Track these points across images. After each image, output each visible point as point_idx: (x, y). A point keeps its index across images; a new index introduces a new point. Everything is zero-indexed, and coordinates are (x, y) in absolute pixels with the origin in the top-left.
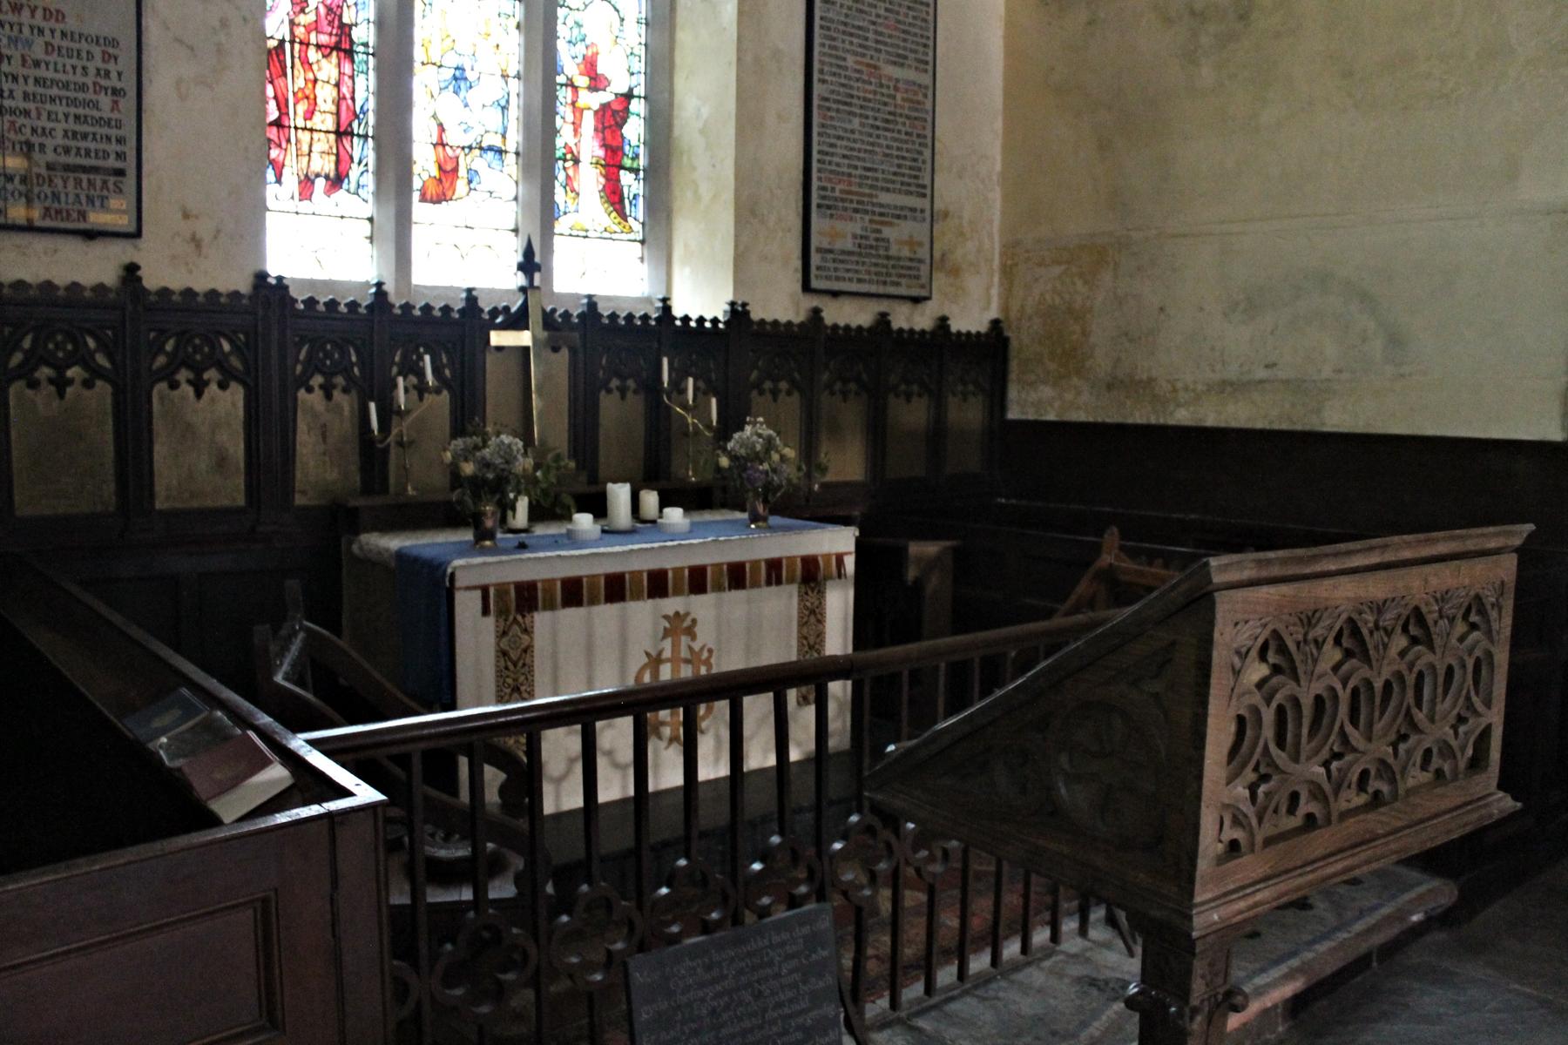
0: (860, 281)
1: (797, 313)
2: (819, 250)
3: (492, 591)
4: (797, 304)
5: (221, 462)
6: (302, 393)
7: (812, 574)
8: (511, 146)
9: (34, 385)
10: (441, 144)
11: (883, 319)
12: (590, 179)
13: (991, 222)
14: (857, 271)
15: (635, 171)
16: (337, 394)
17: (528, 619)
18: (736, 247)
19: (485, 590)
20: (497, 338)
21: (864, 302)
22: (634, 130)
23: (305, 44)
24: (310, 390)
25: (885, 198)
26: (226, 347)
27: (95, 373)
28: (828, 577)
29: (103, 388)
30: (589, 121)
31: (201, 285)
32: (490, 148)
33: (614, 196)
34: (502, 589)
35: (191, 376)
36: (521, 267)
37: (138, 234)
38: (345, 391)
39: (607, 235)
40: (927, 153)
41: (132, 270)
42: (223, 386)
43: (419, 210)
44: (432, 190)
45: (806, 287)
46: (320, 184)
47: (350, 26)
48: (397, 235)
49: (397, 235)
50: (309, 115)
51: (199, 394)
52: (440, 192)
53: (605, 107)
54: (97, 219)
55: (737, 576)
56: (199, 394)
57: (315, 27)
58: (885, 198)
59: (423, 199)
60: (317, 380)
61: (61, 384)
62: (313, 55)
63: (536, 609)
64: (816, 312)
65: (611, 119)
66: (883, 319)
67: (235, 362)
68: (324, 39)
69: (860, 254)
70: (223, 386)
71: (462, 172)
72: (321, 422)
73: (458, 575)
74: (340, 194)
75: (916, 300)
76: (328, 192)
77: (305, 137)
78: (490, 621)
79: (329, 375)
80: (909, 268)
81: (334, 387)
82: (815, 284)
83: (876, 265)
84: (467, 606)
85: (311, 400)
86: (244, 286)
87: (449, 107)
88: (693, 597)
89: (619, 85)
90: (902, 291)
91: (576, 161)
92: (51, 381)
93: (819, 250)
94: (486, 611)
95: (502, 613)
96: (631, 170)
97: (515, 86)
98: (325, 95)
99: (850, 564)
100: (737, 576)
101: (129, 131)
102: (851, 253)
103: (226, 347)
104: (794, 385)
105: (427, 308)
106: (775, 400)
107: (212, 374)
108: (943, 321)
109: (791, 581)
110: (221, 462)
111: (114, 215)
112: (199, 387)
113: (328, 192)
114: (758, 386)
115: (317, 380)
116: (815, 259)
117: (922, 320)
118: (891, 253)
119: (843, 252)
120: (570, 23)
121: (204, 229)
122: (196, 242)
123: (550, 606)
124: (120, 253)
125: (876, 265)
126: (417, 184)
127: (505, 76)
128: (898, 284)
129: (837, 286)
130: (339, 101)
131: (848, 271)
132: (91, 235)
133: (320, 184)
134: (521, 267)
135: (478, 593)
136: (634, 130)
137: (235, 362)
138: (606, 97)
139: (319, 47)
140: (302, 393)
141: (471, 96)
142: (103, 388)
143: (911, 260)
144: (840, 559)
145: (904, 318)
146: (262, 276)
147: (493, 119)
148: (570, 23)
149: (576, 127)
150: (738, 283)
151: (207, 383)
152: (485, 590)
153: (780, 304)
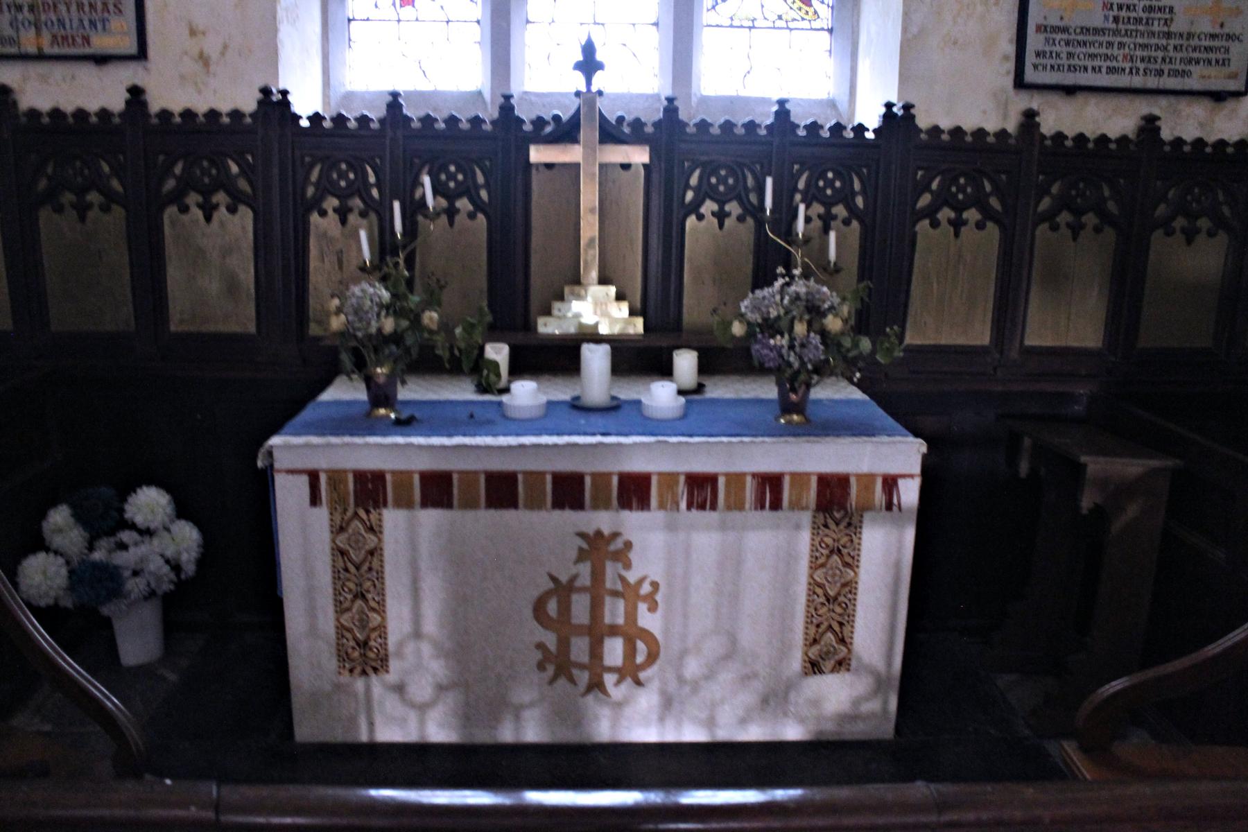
0: (1111, 70)
1: (1005, 117)
2: (1041, 29)
3: (323, 479)
4: (1004, 108)
5: (232, 287)
6: (315, 217)
7: (835, 500)
9: (59, 209)
11: (1150, 124)
14: (1107, 57)
16: (353, 218)
17: (374, 516)
18: (905, 30)
19: (313, 476)
20: (537, 154)
21: (1124, 101)
24: (323, 213)
26: (234, 169)
27: (110, 198)
28: (866, 507)
29: (118, 211)
31: (201, 106)
34: (336, 477)
35: (200, 199)
36: (578, 66)
37: (142, 54)
38: (363, 214)
41: (136, 93)
42: (232, 210)
45: (1020, 83)
51: (208, 219)
54: (102, 43)
55: (701, 490)
56: (208, 219)
60: (331, 203)
61: (82, 210)
63: (385, 504)
64: (1030, 116)
66: (1150, 124)
67: (243, 185)
69: (1116, 32)
70: (232, 210)
73: (276, 454)
75: (1218, 97)
78: (321, 515)
79: (343, 196)
81: (350, 210)
82: (1030, 76)
83: (1144, 47)
84: (289, 495)
85: (323, 224)
86: (248, 103)
88: (626, 514)
90: (1193, 83)
92: (73, 206)
93: (1041, 29)
94: (315, 500)
95: (337, 503)
99: (909, 492)
100: (701, 490)
102: (1096, 31)
103: (234, 169)
104: (988, 214)
105: (452, 121)
106: (957, 235)
107: (221, 198)
109: (796, 505)
110: (232, 287)
111: (119, 38)
112: (209, 211)
114: (930, 213)
116: (1034, 41)
118: (1173, 28)
119: (1085, 30)
121: (211, 46)
122: (203, 59)
123: (404, 502)
124: (126, 75)
125: (1144, 47)
128: (1184, 74)
129: (1069, 79)
131: (1093, 56)
132: (101, 60)
134: (578, 66)
135: (304, 480)
137: (243, 185)
140: (315, 217)
142: (118, 211)
143: (1213, 36)
144: (890, 483)
146: (266, 91)
150: (905, 78)
151: (216, 207)
152: (313, 476)
153: (974, 101)
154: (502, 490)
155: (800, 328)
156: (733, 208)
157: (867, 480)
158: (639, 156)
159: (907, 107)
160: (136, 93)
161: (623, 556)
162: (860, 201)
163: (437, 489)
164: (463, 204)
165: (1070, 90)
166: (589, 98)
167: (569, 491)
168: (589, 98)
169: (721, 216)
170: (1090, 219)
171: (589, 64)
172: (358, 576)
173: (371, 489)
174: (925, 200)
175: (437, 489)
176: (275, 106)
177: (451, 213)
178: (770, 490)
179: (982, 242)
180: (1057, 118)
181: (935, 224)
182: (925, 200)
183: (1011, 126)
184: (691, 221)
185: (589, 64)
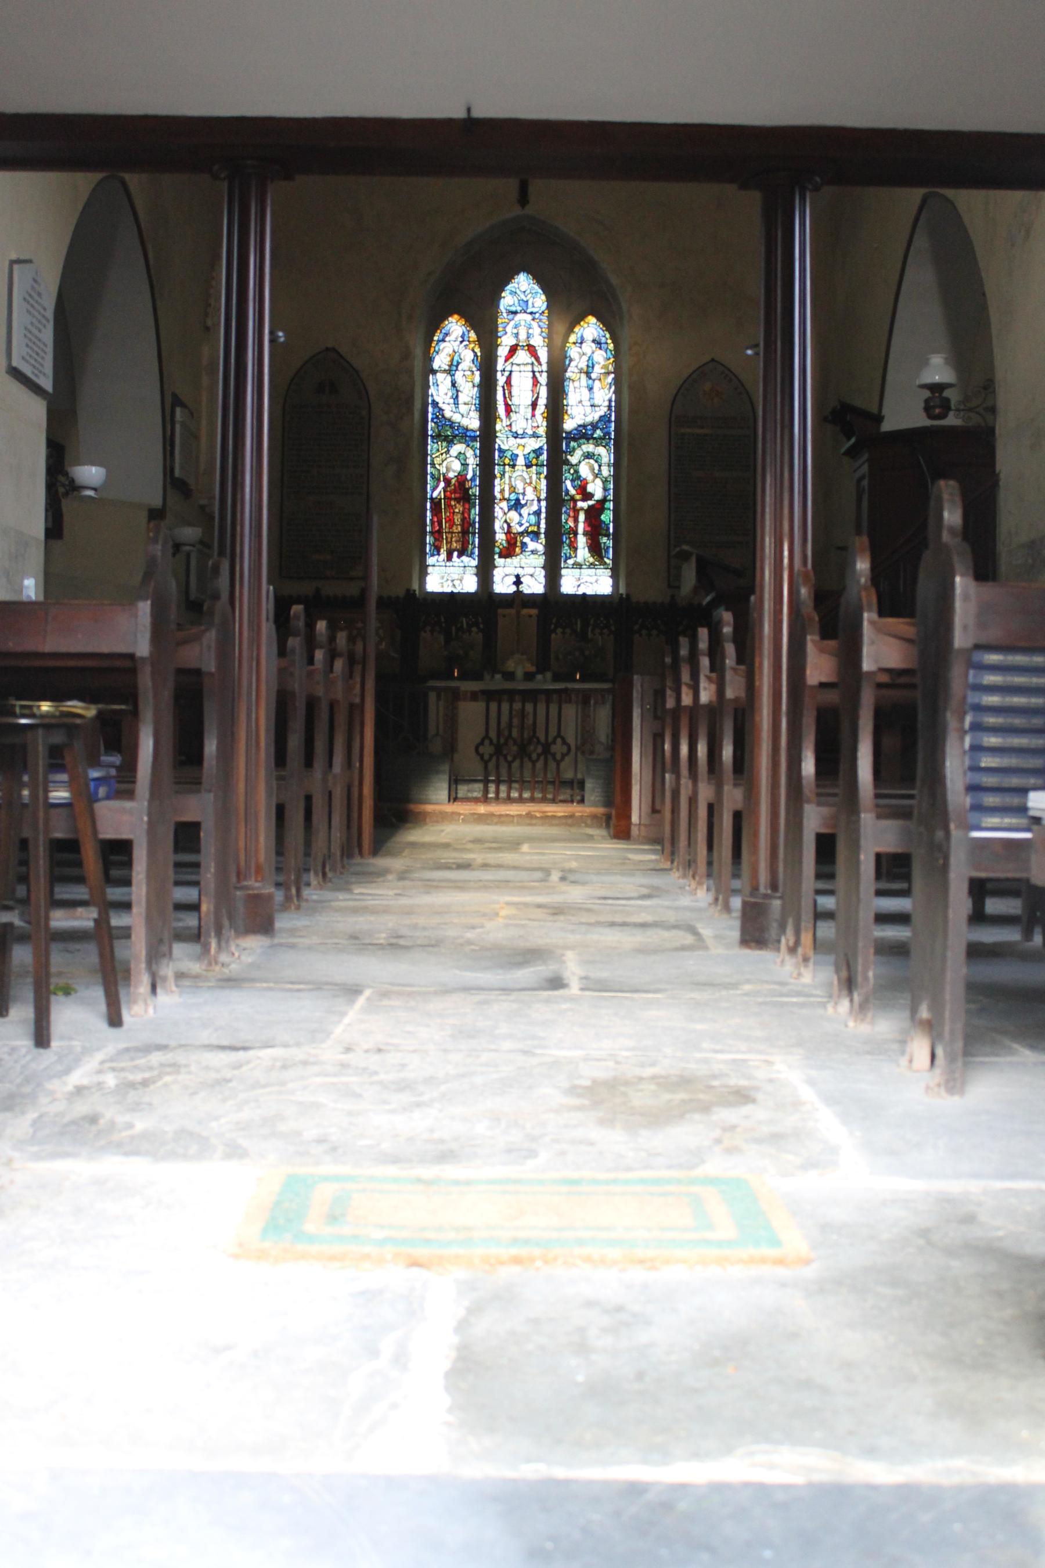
6: (423, 634)
8: (543, 530)
10: (509, 532)
12: (582, 540)
15: (607, 535)
22: (607, 517)
23: (450, 499)
30: (582, 517)
32: (533, 532)
33: (595, 549)
36: (514, 583)
39: (592, 566)
43: (499, 561)
44: (504, 553)
46: (455, 554)
47: (468, 489)
48: (485, 572)
49: (485, 572)
50: (451, 527)
52: (508, 552)
53: (589, 507)
57: (454, 492)
59: (500, 557)
60: (428, 628)
62: (453, 503)
65: (594, 513)
68: (457, 495)
71: (519, 544)
74: (464, 558)
76: (459, 557)
77: (449, 536)
85: (425, 635)
87: (513, 515)
89: (599, 495)
91: (576, 534)
96: (605, 536)
97: (543, 504)
98: (457, 519)
113: (459, 557)
115: (428, 628)
120: (572, 471)
126: (497, 550)
127: (539, 500)
130: (463, 519)
132: (352, 579)
133: (455, 554)
136: (607, 517)
138: (591, 503)
139: (455, 499)
141: (525, 511)
146: (408, 590)
147: (533, 519)
148: (572, 471)
149: (576, 521)
155: (577, 654)
156: (568, 631)
158: (534, 612)
159: (628, 595)
162: (613, 628)
164: (474, 629)
166: (518, 593)
168: (518, 593)
169: (563, 633)
171: (518, 582)
172: (452, 720)
174: (636, 627)
176: (410, 594)
177: (470, 632)
181: (641, 635)
182: (636, 627)
184: (553, 636)
185: (518, 582)
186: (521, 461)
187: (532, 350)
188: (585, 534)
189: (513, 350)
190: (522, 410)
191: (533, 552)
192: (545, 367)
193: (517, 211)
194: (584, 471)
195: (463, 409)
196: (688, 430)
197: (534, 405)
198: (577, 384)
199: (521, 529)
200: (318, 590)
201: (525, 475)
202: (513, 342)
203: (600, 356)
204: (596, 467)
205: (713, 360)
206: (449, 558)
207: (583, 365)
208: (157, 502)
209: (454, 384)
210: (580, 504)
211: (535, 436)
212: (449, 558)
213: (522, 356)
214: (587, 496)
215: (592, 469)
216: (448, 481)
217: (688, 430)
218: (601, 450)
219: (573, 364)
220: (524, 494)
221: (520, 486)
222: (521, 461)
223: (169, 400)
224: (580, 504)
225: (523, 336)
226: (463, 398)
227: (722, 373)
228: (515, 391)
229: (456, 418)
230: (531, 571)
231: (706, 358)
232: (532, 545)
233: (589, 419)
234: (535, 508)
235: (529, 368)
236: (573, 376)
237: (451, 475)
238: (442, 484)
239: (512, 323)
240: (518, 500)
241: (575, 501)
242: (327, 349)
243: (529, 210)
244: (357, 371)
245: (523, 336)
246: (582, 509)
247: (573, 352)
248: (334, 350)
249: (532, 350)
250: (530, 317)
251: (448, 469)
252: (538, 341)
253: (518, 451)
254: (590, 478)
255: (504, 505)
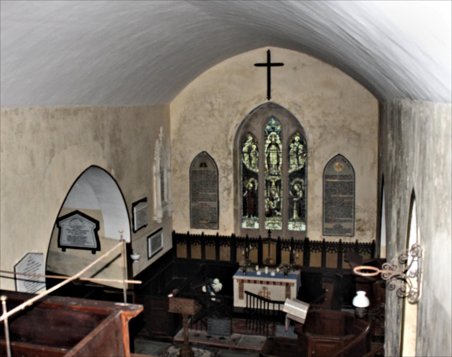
4: (321, 238)
7: (287, 285)
13: (373, 220)
25: (341, 219)
34: (240, 280)
37: (218, 229)
39: (299, 221)
40: (353, 210)
41: (217, 234)
45: (323, 235)
55: (274, 283)
58: (341, 219)
64: (324, 239)
66: (340, 240)
72: (241, 252)
75: (351, 236)
80: (349, 231)
85: (238, 250)
87: (271, 203)
101: (217, 218)
108: (357, 241)
109: (284, 285)
110: (227, 256)
117: (353, 240)
121: (226, 228)
123: (246, 282)
127: (280, 198)
132: (214, 229)
141: (275, 202)
145: (346, 240)
154: (255, 282)
157: (291, 283)
160: (217, 234)
161: (267, 289)
163: (249, 281)
165: (330, 236)
167: (261, 282)
170: (334, 252)
173: (242, 281)
174: (311, 249)
175: (249, 281)
178: (281, 284)
179: (319, 254)
180: (329, 239)
183: (322, 240)
186: (273, 184)
187: (277, 145)
188: (296, 210)
189: (270, 145)
190: (274, 166)
191: (279, 215)
192: (281, 151)
193: (267, 101)
194: (296, 187)
195: (253, 166)
196: (331, 180)
197: (278, 164)
198: (293, 157)
199: (274, 208)
200: (203, 233)
201: (275, 189)
202: (270, 142)
203: (301, 147)
204: (300, 186)
205: (339, 155)
206: (249, 217)
207: (295, 150)
208: (128, 240)
209: (250, 156)
210: (295, 199)
211: (278, 175)
212: (249, 217)
213: (273, 147)
214: (297, 196)
215: (298, 187)
216: (248, 190)
217: (331, 180)
218: (302, 180)
219: (292, 150)
220: (275, 195)
221: (273, 192)
222: (273, 184)
223: (130, 206)
224: (295, 199)
225: (273, 140)
226: (253, 162)
227: (342, 159)
228: (271, 160)
229: (251, 169)
230: (277, 222)
231: (336, 154)
232: (278, 213)
233: (297, 169)
234: (279, 200)
235: (276, 151)
236: (292, 154)
237: (250, 189)
238: (247, 192)
239: (269, 136)
240: (273, 198)
241: (292, 198)
242: (203, 152)
243: (271, 100)
244: (213, 159)
245: (273, 140)
246: (295, 201)
247: (292, 145)
248: (205, 152)
249: (277, 145)
250: (275, 133)
251: (249, 186)
252: (278, 142)
253: (272, 181)
254: (298, 190)
255: (268, 199)
